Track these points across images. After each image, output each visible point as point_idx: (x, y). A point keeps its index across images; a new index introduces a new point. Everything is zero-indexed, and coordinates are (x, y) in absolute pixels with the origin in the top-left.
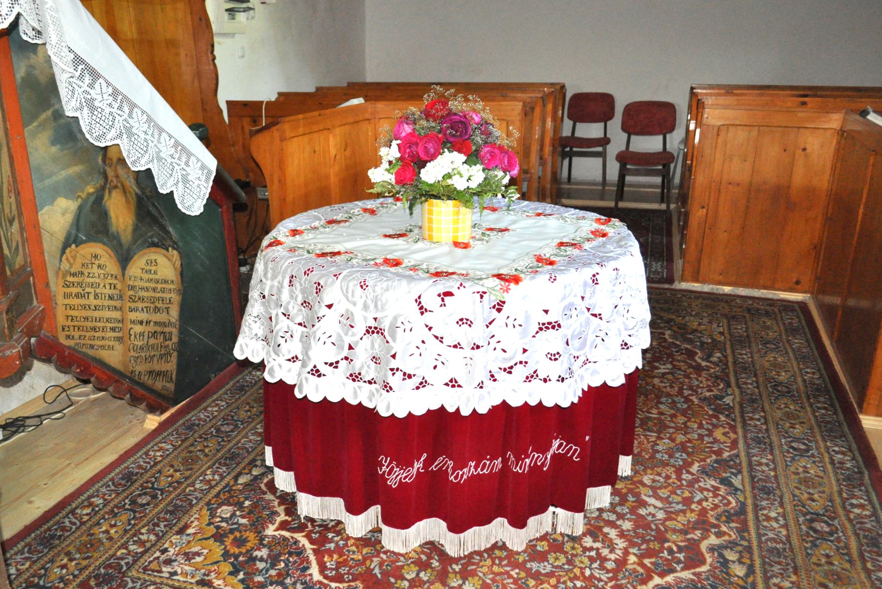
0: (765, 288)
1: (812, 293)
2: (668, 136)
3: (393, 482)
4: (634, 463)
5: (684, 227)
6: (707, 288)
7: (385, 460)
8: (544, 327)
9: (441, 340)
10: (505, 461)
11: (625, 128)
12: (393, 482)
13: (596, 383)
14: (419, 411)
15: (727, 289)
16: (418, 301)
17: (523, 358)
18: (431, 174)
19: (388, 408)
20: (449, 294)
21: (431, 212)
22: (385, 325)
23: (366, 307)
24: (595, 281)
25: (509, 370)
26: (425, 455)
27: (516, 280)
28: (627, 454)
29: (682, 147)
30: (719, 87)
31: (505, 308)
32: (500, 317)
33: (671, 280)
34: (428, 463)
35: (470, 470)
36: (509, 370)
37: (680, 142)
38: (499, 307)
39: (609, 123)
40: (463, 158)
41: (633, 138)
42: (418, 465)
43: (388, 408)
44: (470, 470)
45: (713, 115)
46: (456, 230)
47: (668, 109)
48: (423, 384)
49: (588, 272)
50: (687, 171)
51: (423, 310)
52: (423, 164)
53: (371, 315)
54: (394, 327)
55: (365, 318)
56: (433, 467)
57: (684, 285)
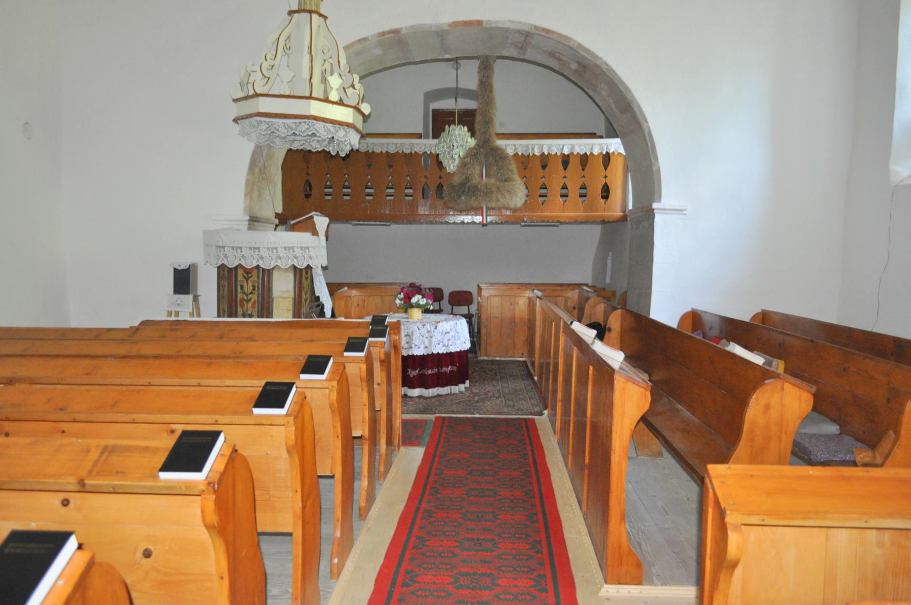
0: (511, 357)
1: (527, 357)
2: (470, 306)
3: (411, 376)
4: (470, 382)
5: (480, 345)
6: (490, 359)
7: (409, 370)
8: (446, 333)
9: (423, 336)
10: (438, 370)
11: (450, 303)
12: (411, 376)
13: (459, 350)
14: (419, 354)
15: (498, 358)
16: (418, 327)
17: (441, 340)
18: (414, 300)
19: (412, 352)
20: (424, 325)
21: (411, 312)
22: (410, 334)
23: (404, 329)
24: (456, 324)
25: (439, 344)
26: (419, 369)
27: (439, 322)
28: (467, 379)
29: (477, 312)
30: (489, 283)
31: (438, 328)
32: (436, 331)
33: (476, 357)
34: (420, 371)
35: (430, 372)
36: (439, 344)
37: (476, 310)
38: (436, 328)
39: (441, 302)
40: (420, 297)
41: (454, 307)
42: (417, 372)
43: (412, 352)
44: (430, 372)
45: (485, 293)
46: (418, 316)
47: (469, 294)
48: (419, 348)
49: (455, 322)
50: (479, 318)
51: (419, 329)
52: (411, 298)
53: (406, 331)
54: (412, 333)
55: (404, 333)
56: (421, 373)
57: (482, 358)
